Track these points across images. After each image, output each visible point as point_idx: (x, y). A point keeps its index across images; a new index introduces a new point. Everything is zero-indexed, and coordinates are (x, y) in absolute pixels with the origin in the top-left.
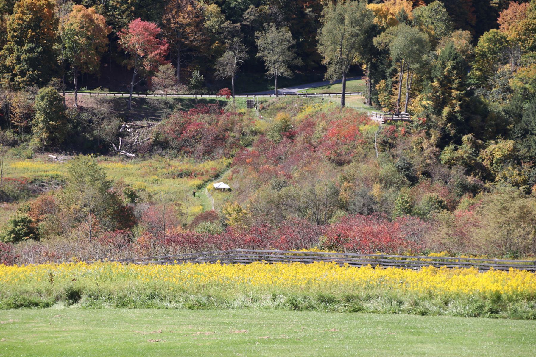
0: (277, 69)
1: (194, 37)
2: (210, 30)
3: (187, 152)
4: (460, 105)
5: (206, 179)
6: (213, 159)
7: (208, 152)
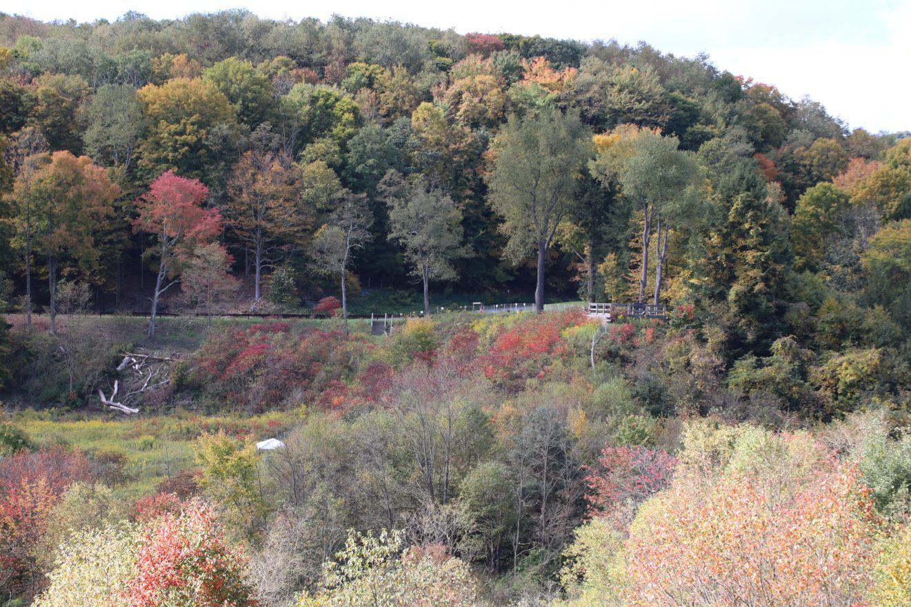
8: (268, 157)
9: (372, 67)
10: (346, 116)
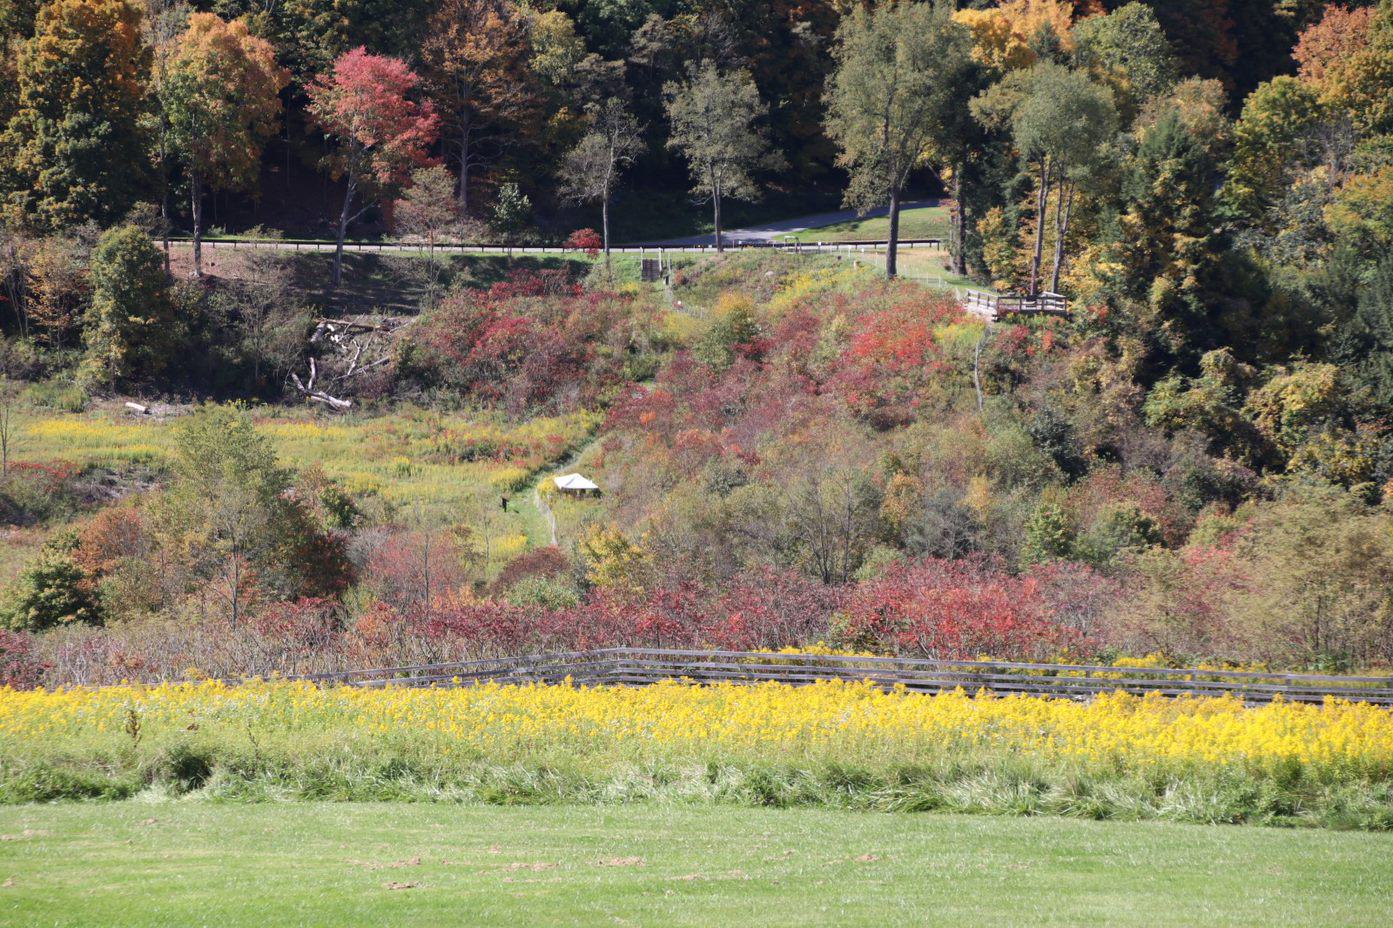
0: (718, 180)
1: (504, 97)
2: (545, 77)
3: (485, 396)
4: (1196, 273)
5: (534, 466)
6: (553, 413)
7: (541, 396)
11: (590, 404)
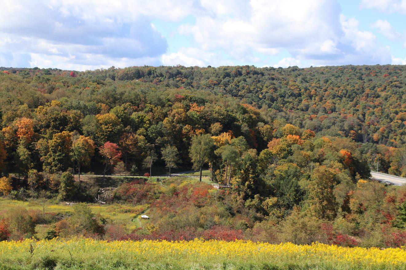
0: (171, 165)
1: (133, 150)
2: (140, 147)
3: (129, 202)
4: (253, 181)
5: (138, 214)
6: (141, 204)
7: (139, 202)
8: (129, 135)
9: (152, 105)
10: (147, 122)
11: (147, 203)
